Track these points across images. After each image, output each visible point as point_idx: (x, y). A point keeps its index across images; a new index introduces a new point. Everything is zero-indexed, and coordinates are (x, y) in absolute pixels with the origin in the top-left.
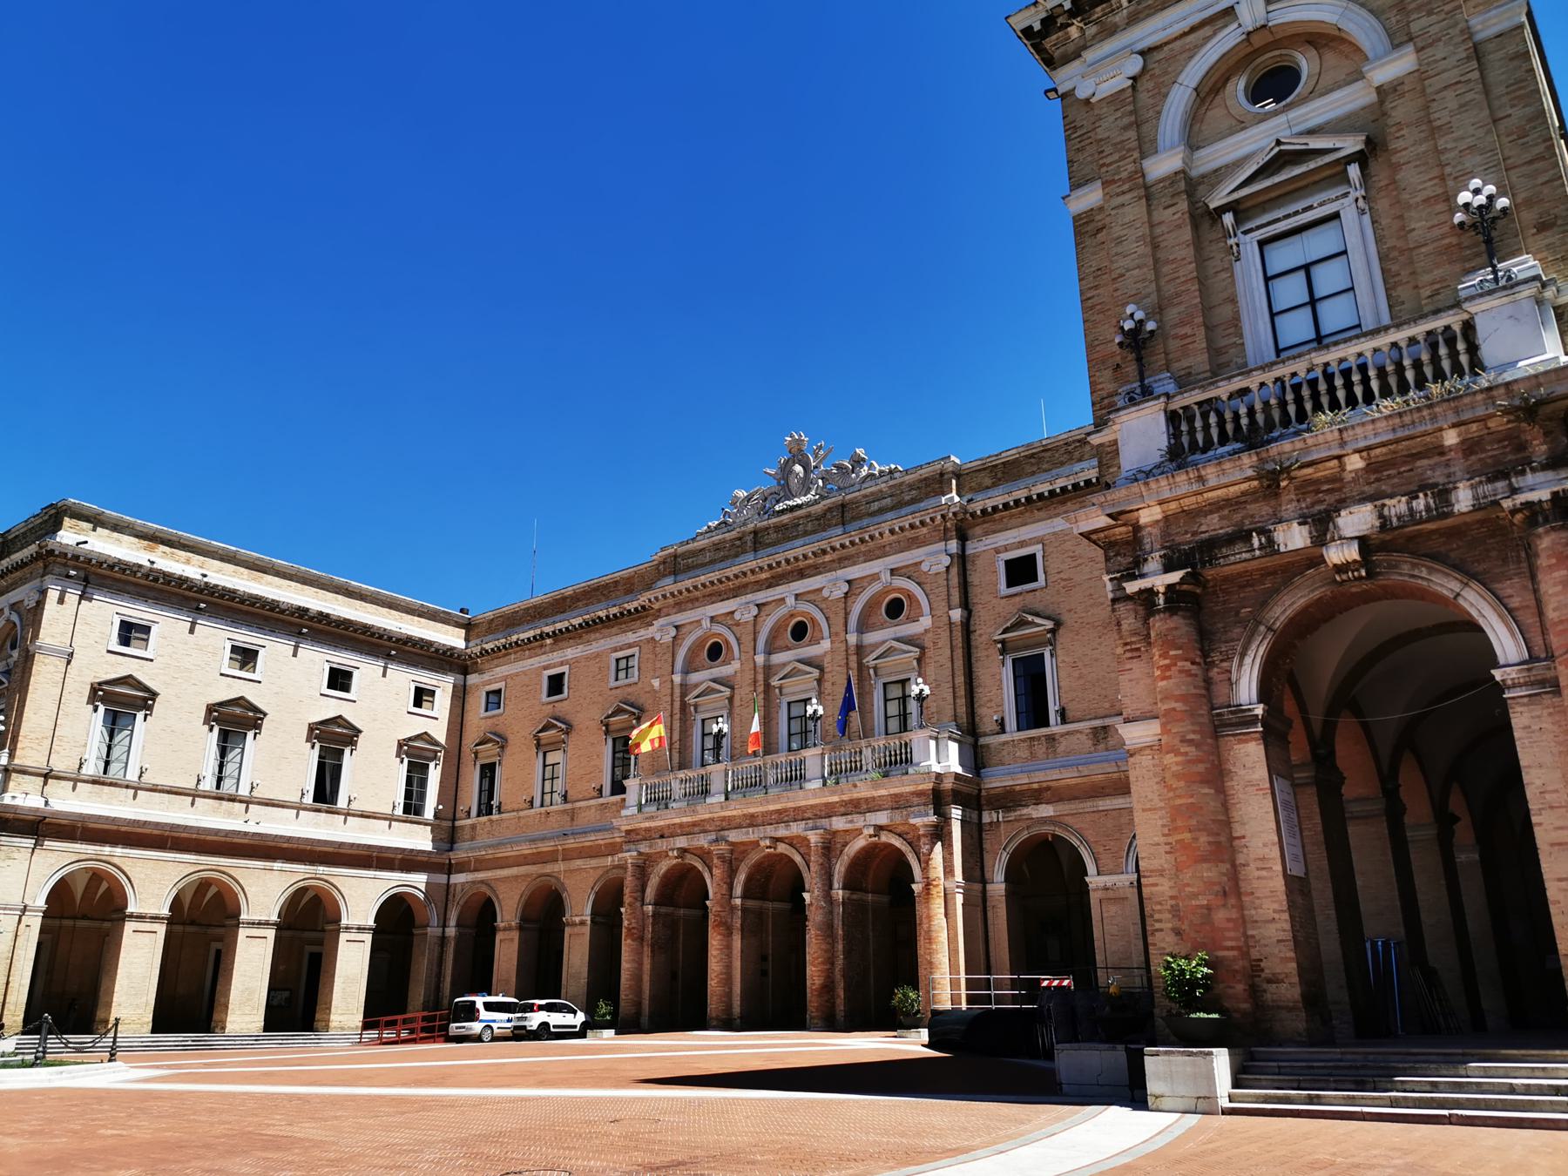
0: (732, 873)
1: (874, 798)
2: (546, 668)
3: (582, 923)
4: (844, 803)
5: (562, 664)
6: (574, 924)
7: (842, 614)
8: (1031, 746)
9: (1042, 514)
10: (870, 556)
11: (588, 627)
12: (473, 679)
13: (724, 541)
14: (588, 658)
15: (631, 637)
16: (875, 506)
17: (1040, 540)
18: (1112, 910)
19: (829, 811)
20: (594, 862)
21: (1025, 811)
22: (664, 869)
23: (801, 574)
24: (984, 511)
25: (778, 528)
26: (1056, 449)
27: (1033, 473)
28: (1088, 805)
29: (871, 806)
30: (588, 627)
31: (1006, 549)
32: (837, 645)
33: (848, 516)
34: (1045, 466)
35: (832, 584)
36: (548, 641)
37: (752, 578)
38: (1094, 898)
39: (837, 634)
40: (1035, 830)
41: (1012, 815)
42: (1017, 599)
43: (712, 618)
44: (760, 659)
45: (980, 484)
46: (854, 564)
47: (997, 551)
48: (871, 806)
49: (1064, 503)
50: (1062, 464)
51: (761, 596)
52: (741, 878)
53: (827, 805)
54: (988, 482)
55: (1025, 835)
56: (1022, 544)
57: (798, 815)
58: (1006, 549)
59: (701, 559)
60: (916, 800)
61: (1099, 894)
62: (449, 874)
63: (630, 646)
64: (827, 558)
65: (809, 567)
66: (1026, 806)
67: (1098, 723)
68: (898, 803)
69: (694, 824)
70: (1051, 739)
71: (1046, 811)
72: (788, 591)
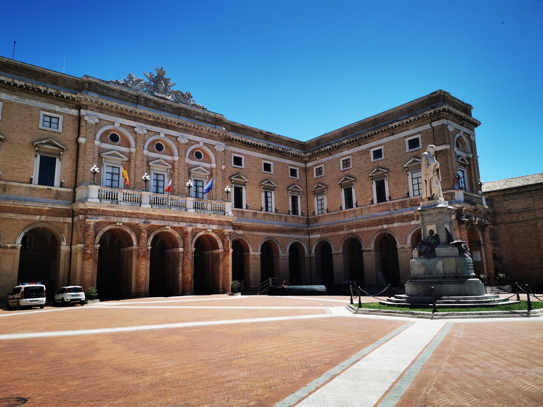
0: (148, 236)
1: (212, 220)
3: (14, 248)
4: (201, 219)
7: (184, 150)
8: (238, 213)
9: (244, 147)
10: (196, 134)
13: (127, 93)
14: (19, 105)
15: (57, 108)
16: (197, 117)
18: (255, 261)
19: (196, 221)
20: (24, 217)
22: (127, 230)
23: (168, 127)
24: (233, 139)
25: (155, 102)
26: (249, 130)
28: (251, 233)
29: (211, 222)
32: (181, 160)
35: (184, 138)
37: (145, 118)
38: (251, 257)
39: (182, 156)
40: (238, 237)
43: (204, 143)
46: (190, 134)
47: (232, 152)
48: (211, 222)
49: (250, 147)
51: (149, 127)
52: (151, 238)
53: (195, 219)
54: (230, 129)
56: (239, 153)
57: (183, 220)
58: (234, 153)
59: (111, 93)
60: (226, 224)
61: (252, 257)
63: (55, 112)
64: (180, 127)
65: (172, 126)
67: (255, 211)
68: (220, 223)
69: (133, 214)
70: (243, 212)
71: (241, 232)
72: (163, 131)
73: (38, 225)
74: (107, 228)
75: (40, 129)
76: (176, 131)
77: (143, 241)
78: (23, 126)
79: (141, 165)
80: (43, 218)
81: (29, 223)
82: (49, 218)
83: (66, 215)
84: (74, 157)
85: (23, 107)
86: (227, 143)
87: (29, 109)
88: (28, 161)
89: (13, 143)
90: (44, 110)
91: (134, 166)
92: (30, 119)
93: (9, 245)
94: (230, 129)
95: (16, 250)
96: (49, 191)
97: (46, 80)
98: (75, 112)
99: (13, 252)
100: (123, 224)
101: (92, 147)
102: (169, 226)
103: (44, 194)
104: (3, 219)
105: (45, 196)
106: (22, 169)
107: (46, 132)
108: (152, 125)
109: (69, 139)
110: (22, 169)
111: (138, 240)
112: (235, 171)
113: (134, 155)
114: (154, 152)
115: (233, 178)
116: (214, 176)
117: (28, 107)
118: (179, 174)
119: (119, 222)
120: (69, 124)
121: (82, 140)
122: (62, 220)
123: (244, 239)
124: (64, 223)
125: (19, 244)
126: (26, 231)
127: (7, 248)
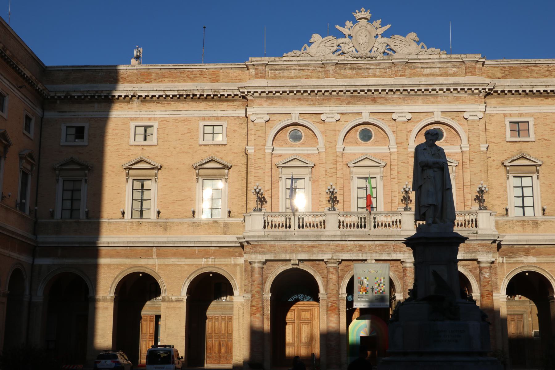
2: (132, 119)
3: (179, 300)
5: (150, 119)
6: (170, 301)
8: (523, 225)
11: (180, 98)
12: (49, 115)
14: (176, 120)
17: (532, 115)
21: (519, 259)
27: (528, 77)
30: (180, 98)
31: (511, 115)
33: (408, 72)
34: (535, 75)
36: (136, 101)
39: (402, 143)
41: (512, 260)
42: (517, 144)
44: (340, 146)
45: (494, 75)
47: (505, 115)
50: (546, 76)
54: (500, 75)
55: (519, 271)
56: (521, 115)
60: (480, 248)
62: (34, 257)
63: (217, 118)
66: (521, 257)
71: (532, 260)
73: (205, 271)
74: (281, 268)
75: (200, 145)
76: (389, 103)
77: (331, 286)
78: (182, 145)
79: (334, 170)
80: (210, 261)
81: (195, 269)
82: (216, 260)
83: (237, 254)
84: (244, 175)
85: (179, 121)
86: (492, 101)
87: (186, 123)
88: (189, 189)
89: (171, 169)
90: (204, 119)
91: (324, 173)
92: (189, 135)
93: (174, 298)
94: (500, 75)
95: (181, 303)
96: (215, 224)
97: (204, 79)
98: (241, 113)
99: (179, 306)
100: (300, 260)
101: (263, 156)
102: (372, 259)
103: (210, 229)
104: (166, 265)
105: (210, 231)
106: (183, 200)
107: (207, 148)
108: (348, 104)
109: (235, 151)
110: (183, 200)
111: (327, 283)
112: (514, 151)
113: (323, 156)
114: (357, 144)
115: (506, 163)
116: (467, 165)
117: (186, 120)
118: (398, 173)
119: (294, 260)
120: (234, 131)
121: (250, 150)
122: (232, 261)
123: (539, 271)
124: (236, 265)
125: (184, 295)
126: (192, 278)
127: (172, 301)
